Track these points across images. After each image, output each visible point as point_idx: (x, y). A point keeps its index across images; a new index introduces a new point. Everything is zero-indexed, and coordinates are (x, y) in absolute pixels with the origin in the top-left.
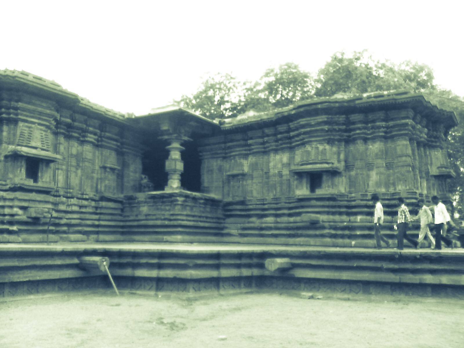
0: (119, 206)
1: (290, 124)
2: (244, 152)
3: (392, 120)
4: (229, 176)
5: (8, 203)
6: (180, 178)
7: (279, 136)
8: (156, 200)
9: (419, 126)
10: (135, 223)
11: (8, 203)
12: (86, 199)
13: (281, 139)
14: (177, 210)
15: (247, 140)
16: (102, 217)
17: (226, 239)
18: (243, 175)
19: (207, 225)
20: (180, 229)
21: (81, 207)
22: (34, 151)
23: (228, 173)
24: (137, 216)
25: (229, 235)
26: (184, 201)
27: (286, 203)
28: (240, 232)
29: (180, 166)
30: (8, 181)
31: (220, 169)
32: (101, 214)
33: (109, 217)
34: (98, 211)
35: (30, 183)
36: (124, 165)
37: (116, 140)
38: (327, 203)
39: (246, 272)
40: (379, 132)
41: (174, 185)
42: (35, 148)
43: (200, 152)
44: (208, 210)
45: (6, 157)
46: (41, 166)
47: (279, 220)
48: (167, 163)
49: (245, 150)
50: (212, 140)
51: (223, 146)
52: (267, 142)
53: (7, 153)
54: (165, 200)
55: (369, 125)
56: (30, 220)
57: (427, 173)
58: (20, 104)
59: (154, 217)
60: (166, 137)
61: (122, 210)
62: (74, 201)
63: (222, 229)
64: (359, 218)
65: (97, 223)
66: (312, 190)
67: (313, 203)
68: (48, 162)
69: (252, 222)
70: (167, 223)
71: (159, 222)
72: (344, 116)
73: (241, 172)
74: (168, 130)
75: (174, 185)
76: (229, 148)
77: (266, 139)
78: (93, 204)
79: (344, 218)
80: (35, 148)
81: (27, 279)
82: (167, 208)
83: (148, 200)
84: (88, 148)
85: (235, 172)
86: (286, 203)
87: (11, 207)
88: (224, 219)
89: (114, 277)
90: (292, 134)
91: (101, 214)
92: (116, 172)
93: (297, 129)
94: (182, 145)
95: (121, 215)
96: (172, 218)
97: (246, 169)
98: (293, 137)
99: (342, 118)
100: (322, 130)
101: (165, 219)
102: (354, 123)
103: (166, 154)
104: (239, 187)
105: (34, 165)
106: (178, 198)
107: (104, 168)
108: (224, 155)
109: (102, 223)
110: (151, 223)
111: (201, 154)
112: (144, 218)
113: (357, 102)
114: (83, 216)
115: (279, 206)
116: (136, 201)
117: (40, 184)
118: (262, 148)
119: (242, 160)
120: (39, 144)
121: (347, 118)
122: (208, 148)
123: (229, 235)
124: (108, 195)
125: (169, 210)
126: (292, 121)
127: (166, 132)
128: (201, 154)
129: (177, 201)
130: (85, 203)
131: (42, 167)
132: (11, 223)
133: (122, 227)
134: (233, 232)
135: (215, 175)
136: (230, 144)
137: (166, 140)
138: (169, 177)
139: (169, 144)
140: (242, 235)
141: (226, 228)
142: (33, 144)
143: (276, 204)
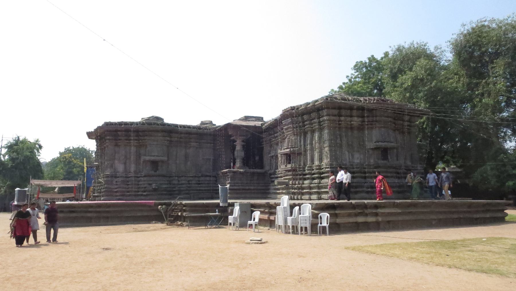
21: (189, 181)
22: (152, 158)
29: (242, 154)
33: (207, 185)
35: (152, 173)
40: (315, 126)
41: (238, 164)
58: (146, 138)
60: (232, 138)
65: (198, 188)
68: (162, 162)
78: (197, 179)
79: (301, 182)
87: (144, 184)
99: (300, 119)
102: (306, 121)
105: (155, 164)
109: (201, 188)
114: (189, 186)
117: (158, 173)
120: (156, 154)
130: (191, 178)
131: (160, 164)
132: (145, 192)
139: (236, 141)
142: (153, 154)
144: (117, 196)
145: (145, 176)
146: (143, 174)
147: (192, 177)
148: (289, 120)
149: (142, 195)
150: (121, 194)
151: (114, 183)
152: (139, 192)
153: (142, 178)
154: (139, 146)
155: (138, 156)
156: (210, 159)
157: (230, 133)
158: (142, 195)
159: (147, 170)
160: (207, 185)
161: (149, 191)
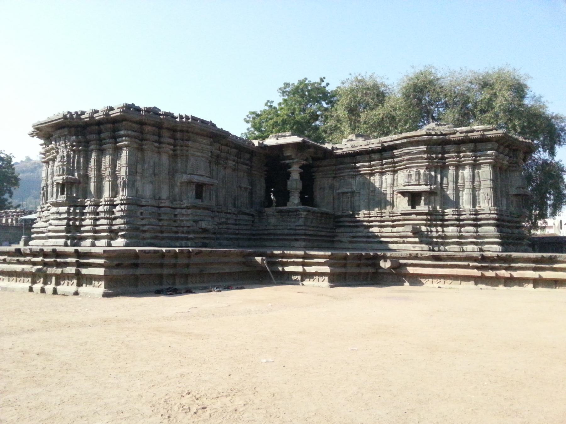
0: (250, 218)
1: (394, 151)
2: (352, 173)
3: (480, 151)
4: (339, 194)
5: (184, 218)
6: (299, 195)
7: (384, 161)
8: (282, 214)
9: (501, 155)
10: (266, 232)
11: (184, 218)
12: (230, 213)
13: (386, 164)
14: (301, 222)
15: (355, 163)
16: (241, 227)
17: (336, 245)
18: (353, 193)
19: (323, 234)
20: (303, 237)
23: (337, 191)
24: (266, 226)
25: (341, 242)
26: (307, 214)
27: (390, 216)
28: (349, 239)
29: (300, 185)
30: (184, 201)
31: (332, 187)
32: (239, 224)
34: (237, 223)
35: (199, 202)
36: (252, 183)
37: (247, 165)
38: (425, 217)
39: (364, 270)
41: (295, 200)
42: (202, 176)
43: (313, 172)
44: (323, 221)
45: (181, 183)
46: (204, 188)
47: (383, 230)
48: (289, 183)
49: (354, 172)
50: (325, 163)
51: (334, 168)
52: (373, 165)
53: (183, 180)
54: (290, 214)
55: (461, 154)
56: (200, 230)
57: (508, 194)
58: (190, 143)
59: (281, 227)
60: (287, 162)
61: (253, 222)
62: (223, 215)
63: (334, 237)
64: (451, 229)
66: (413, 207)
67: (413, 216)
69: (360, 232)
70: (293, 232)
71: (286, 232)
72: (440, 146)
73: (350, 190)
74: (291, 156)
75: (295, 200)
76: (339, 169)
77: (372, 163)
80: (202, 176)
81: (218, 272)
82: (293, 220)
83: (275, 214)
84: (229, 171)
85: (345, 190)
86: (390, 216)
88: (335, 229)
89: (272, 272)
90: (396, 160)
91: (239, 224)
92: (248, 190)
93: (401, 156)
94: (300, 168)
95: (252, 226)
96: (297, 228)
97: (354, 188)
98: (397, 162)
100: (422, 157)
101: (291, 229)
102: (448, 153)
103: (288, 175)
104: (348, 202)
105: (200, 189)
106: (302, 212)
107: (240, 187)
108: (334, 175)
110: (279, 232)
111: (313, 174)
112: (273, 228)
113: (451, 136)
115: (384, 218)
116: (265, 214)
118: (368, 170)
119: (350, 180)
120: (203, 173)
121: (443, 148)
122: (321, 169)
123: (341, 242)
124: (244, 209)
125: (294, 222)
126: (396, 149)
127: (289, 158)
128: (313, 174)
129: (301, 214)
130: (229, 216)
132: (188, 232)
133: (254, 235)
134: (344, 239)
135: (326, 191)
136: (341, 166)
137: (288, 164)
138: (290, 194)
139: (290, 168)
140: (350, 242)
141: (337, 236)
142: (200, 172)
143: (382, 217)
144: (144, 239)
145: (188, 208)
146: (185, 203)
147: (230, 213)
148: (423, 148)
149: (182, 239)
150: (153, 235)
151: (139, 213)
152: (177, 232)
153: (183, 211)
154: (174, 156)
155: (173, 173)
156: (247, 188)
157: (289, 154)
158: (182, 239)
159: (189, 198)
160: (245, 228)
161: (194, 232)
